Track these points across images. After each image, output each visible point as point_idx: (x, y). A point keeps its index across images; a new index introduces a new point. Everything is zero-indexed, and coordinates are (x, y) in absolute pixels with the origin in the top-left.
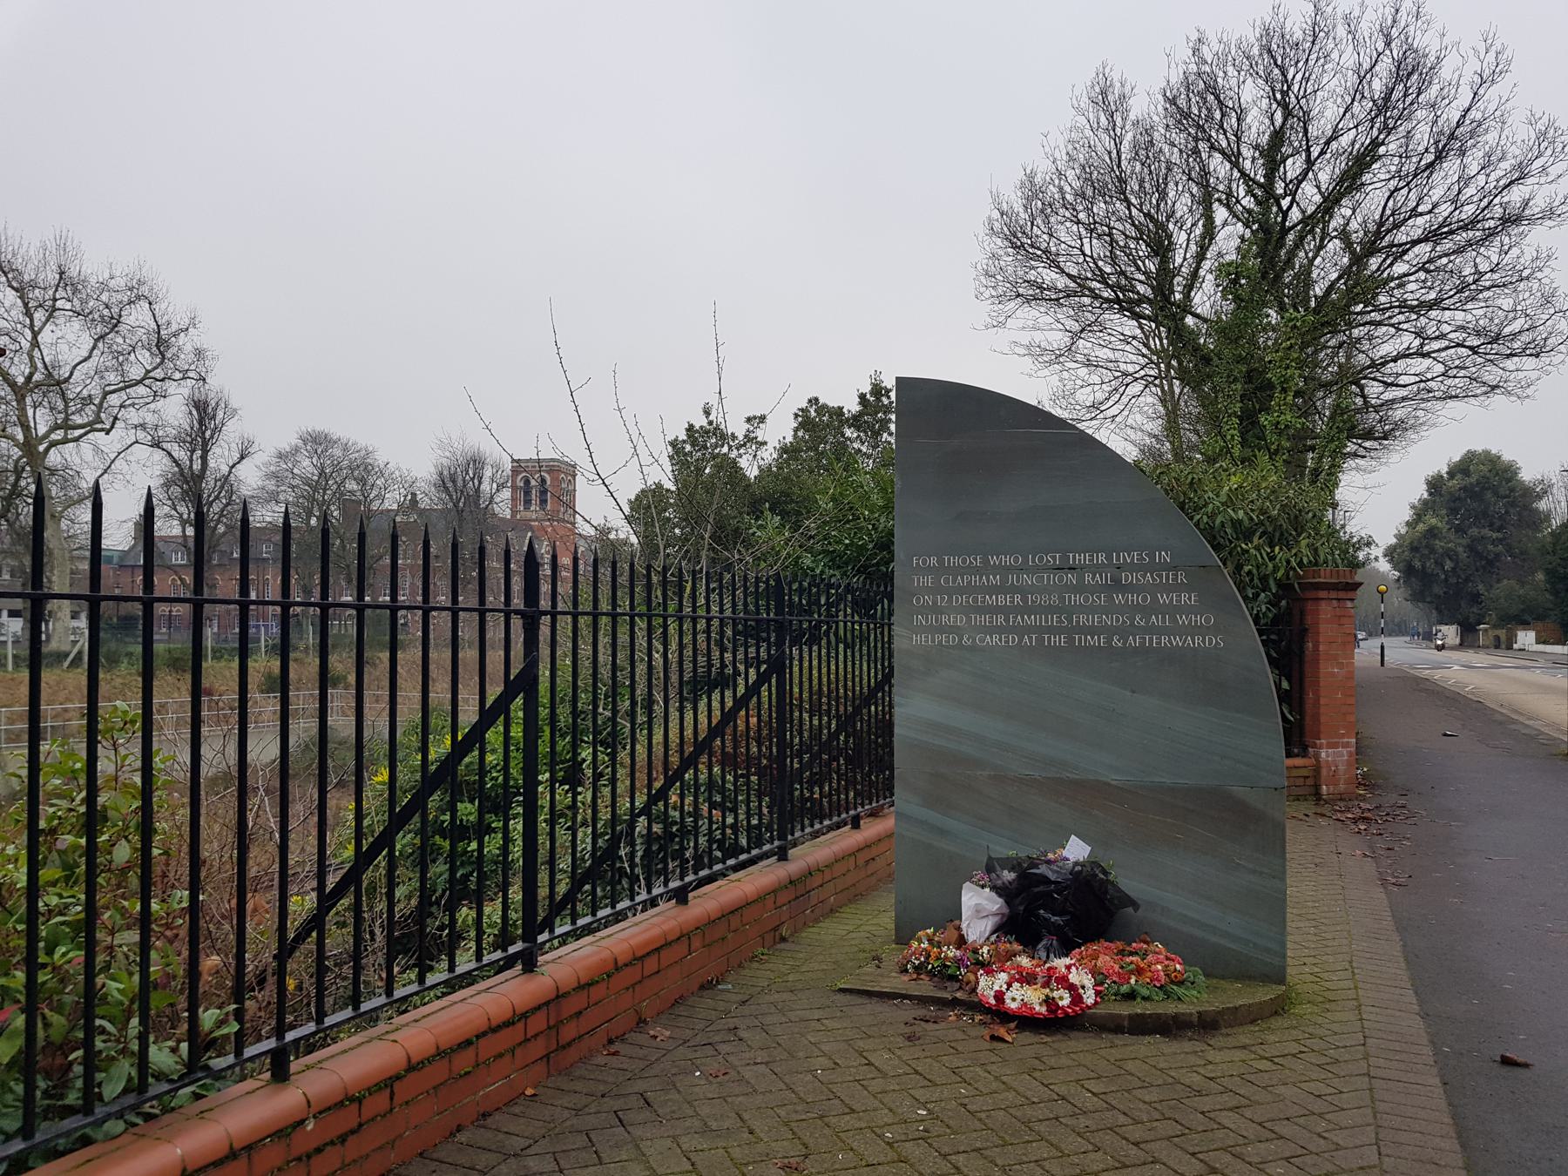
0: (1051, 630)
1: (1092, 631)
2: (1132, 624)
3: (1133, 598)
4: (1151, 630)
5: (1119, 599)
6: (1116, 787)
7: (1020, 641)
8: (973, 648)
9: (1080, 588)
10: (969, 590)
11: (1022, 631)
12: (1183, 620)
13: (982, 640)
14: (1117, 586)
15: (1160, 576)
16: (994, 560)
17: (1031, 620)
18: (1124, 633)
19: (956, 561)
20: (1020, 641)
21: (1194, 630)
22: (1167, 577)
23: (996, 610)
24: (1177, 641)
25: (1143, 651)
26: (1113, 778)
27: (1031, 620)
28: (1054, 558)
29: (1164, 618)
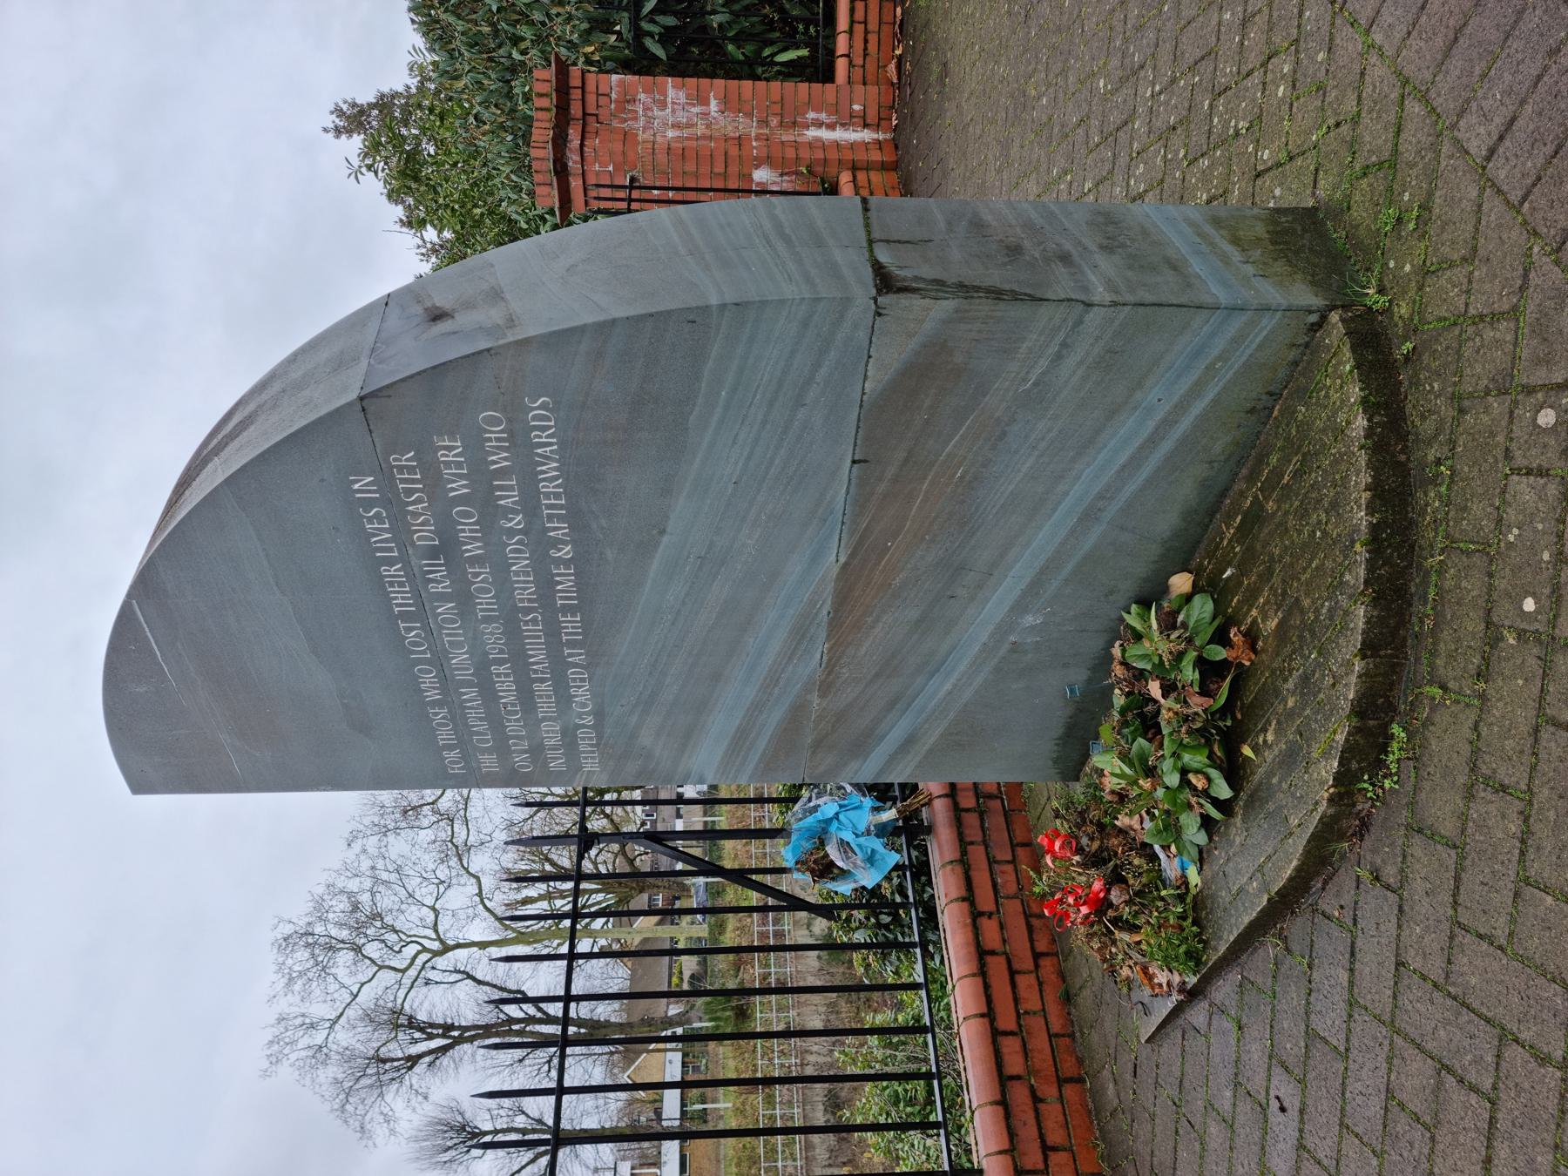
0: (553, 633)
1: (546, 586)
2: (520, 532)
3: (467, 528)
4: (530, 504)
5: (473, 549)
6: (852, 556)
7: (576, 665)
8: (599, 714)
9: (464, 598)
10: (496, 722)
11: (559, 668)
12: (500, 460)
13: (584, 705)
14: (446, 549)
15: (410, 492)
16: (433, 695)
17: (538, 656)
18: (540, 544)
19: (444, 735)
20: (576, 665)
21: (518, 438)
22: (409, 482)
23: (527, 699)
24: (550, 469)
25: (575, 517)
26: (833, 560)
27: (538, 656)
28: (410, 629)
29: (501, 488)
